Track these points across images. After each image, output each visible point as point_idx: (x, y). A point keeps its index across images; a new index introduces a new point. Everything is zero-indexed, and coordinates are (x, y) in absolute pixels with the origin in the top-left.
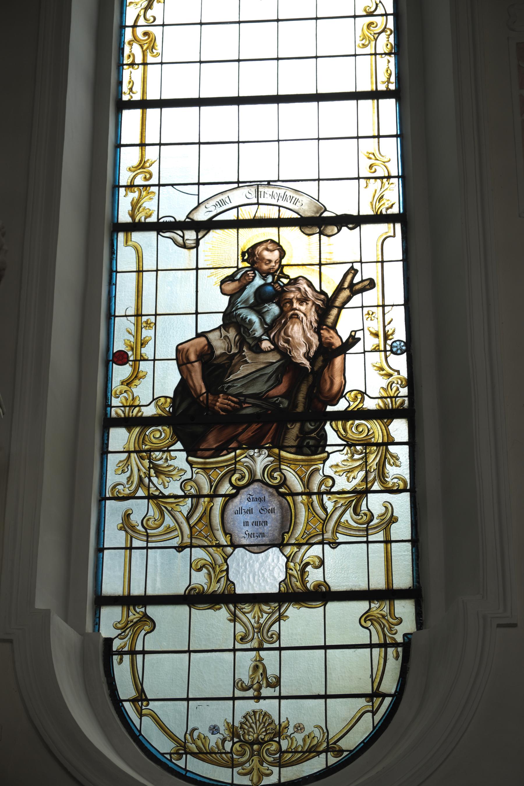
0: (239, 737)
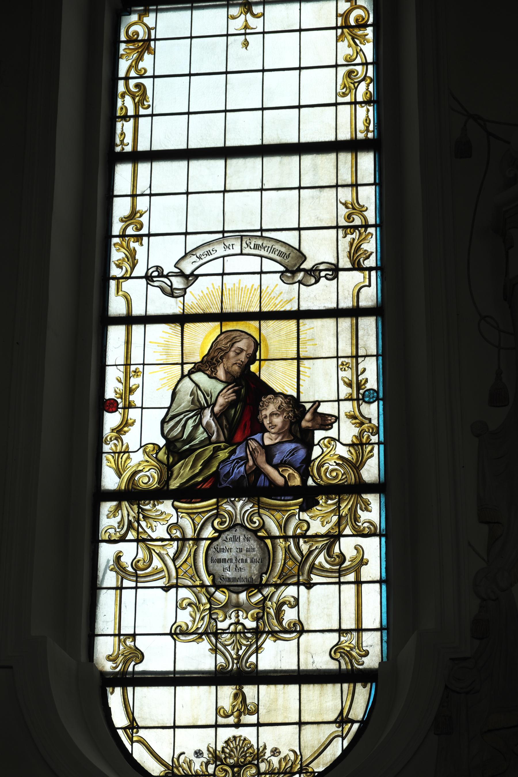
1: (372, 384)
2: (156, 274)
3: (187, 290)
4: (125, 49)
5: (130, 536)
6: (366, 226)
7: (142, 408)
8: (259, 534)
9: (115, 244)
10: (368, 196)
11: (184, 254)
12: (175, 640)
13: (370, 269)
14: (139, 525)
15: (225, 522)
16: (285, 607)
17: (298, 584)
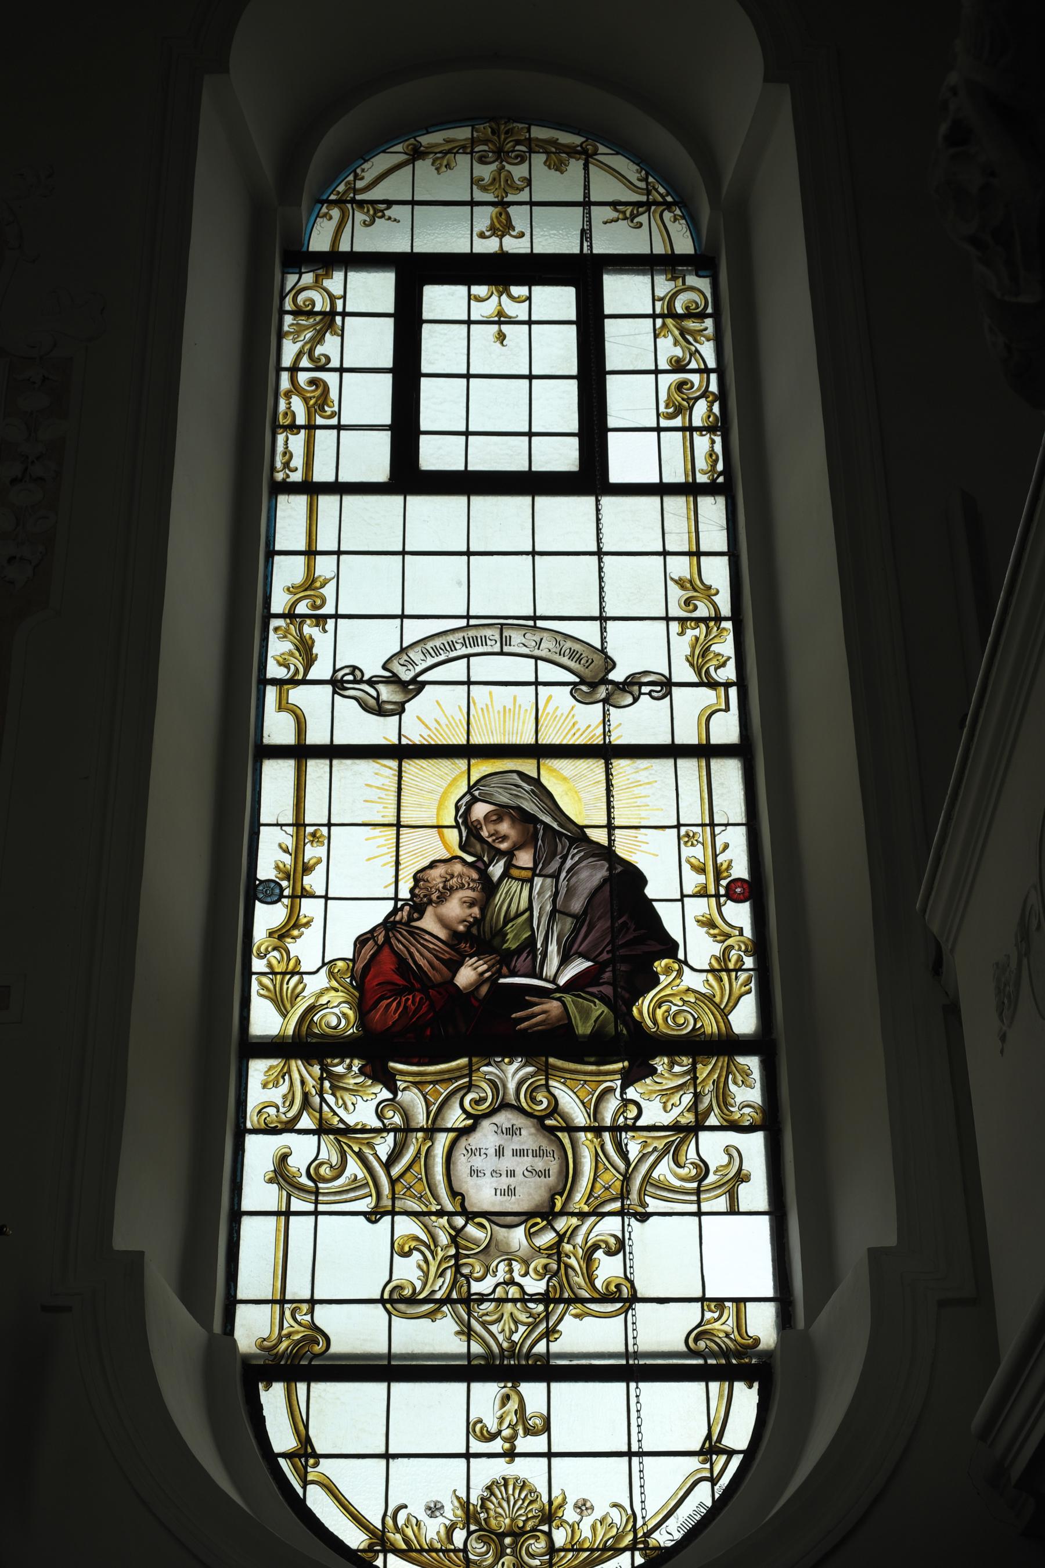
0: (478, 1522)
1: (741, 870)
2: (350, 678)
3: (407, 706)
4: (293, 324)
5: (306, 1122)
6: (718, 619)
7: (326, 898)
8: (548, 1122)
9: (276, 629)
10: (717, 573)
11: (398, 649)
12: (389, 1313)
13: (727, 685)
14: (323, 1100)
15: (485, 1099)
16: (599, 1254)
17: (621, 1213)
